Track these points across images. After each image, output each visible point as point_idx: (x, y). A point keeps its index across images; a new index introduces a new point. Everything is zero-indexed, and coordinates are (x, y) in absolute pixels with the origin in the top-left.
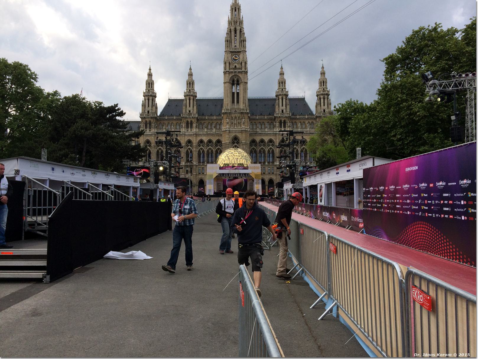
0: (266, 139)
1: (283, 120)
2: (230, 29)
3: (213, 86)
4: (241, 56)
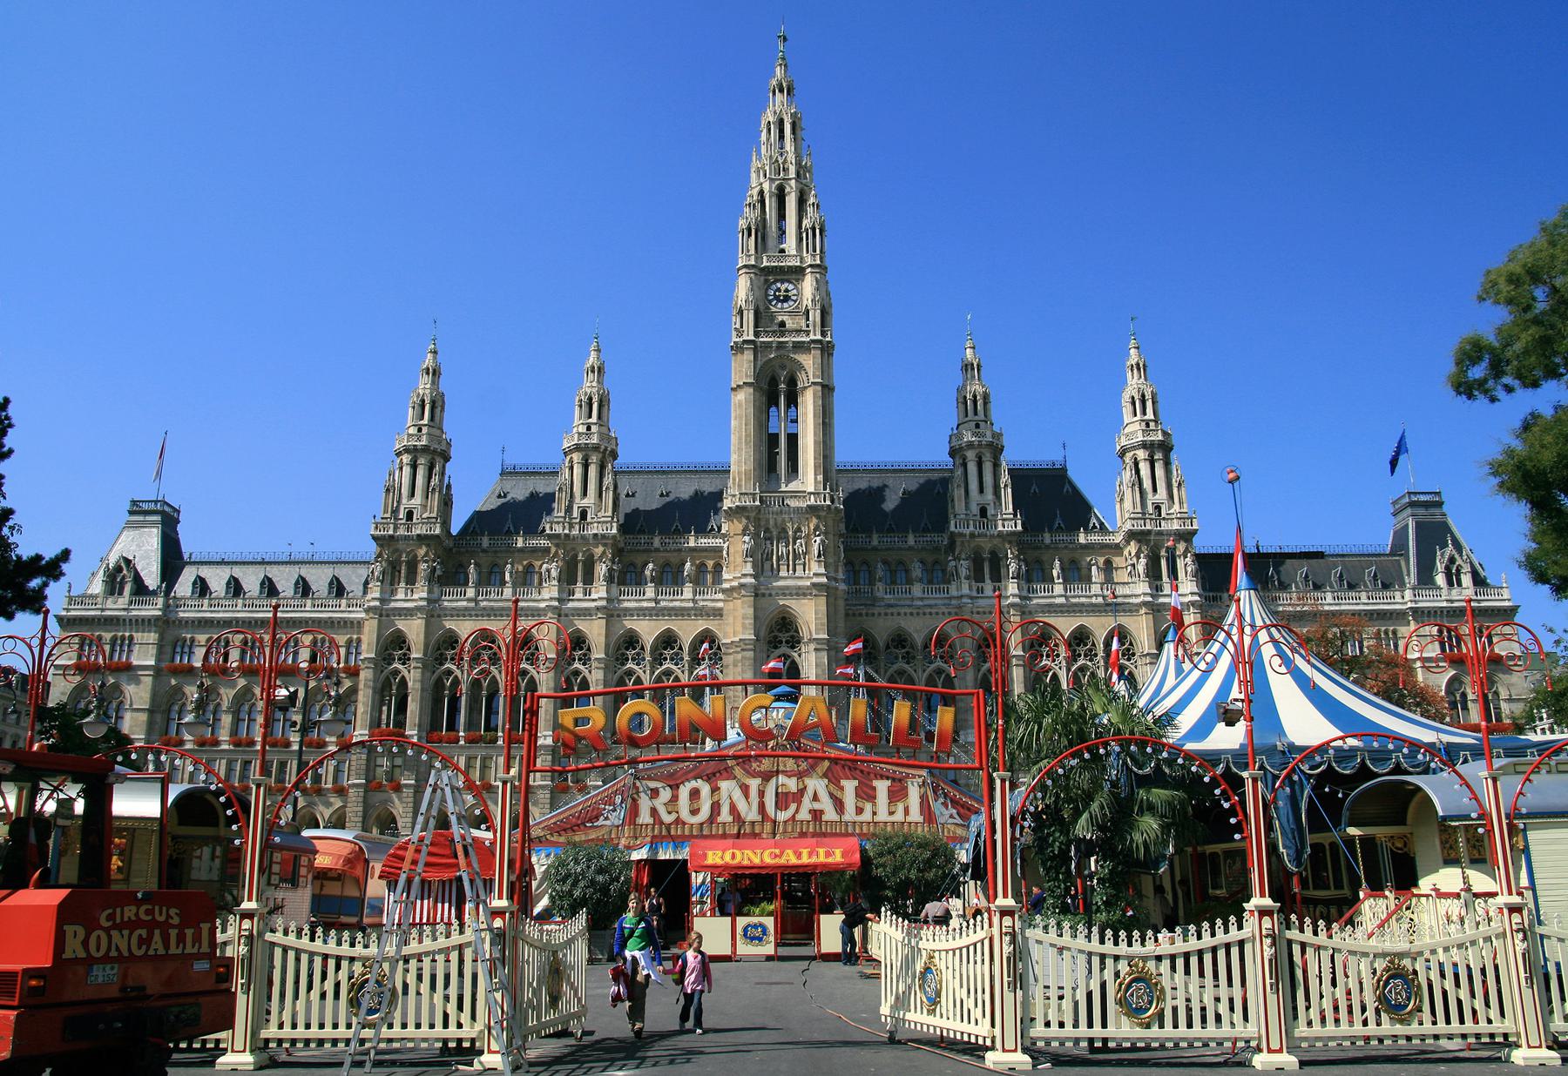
0: (917, 628)
1: (987, 546)
2: (761, 193)
4: (808, 285)
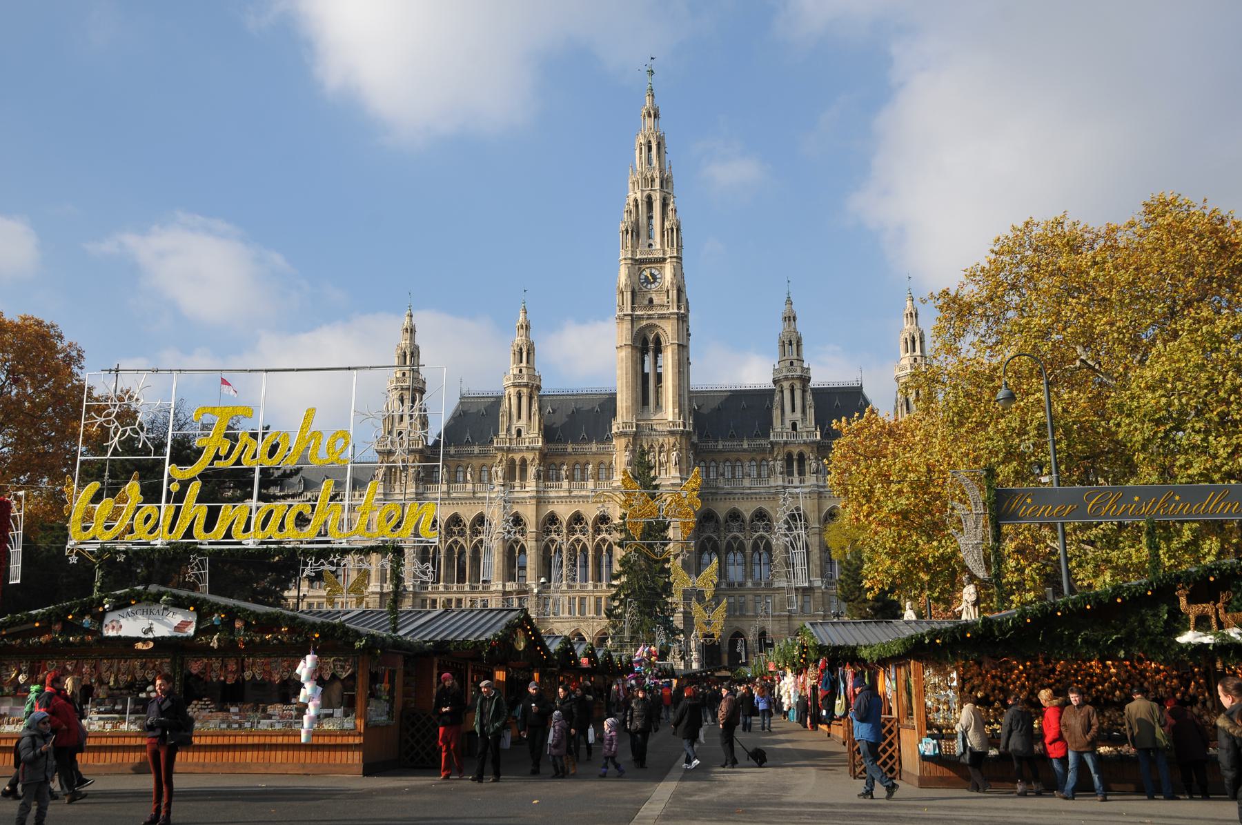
0: (747, 509)
2: (636, 201)
3: (590, 357)
